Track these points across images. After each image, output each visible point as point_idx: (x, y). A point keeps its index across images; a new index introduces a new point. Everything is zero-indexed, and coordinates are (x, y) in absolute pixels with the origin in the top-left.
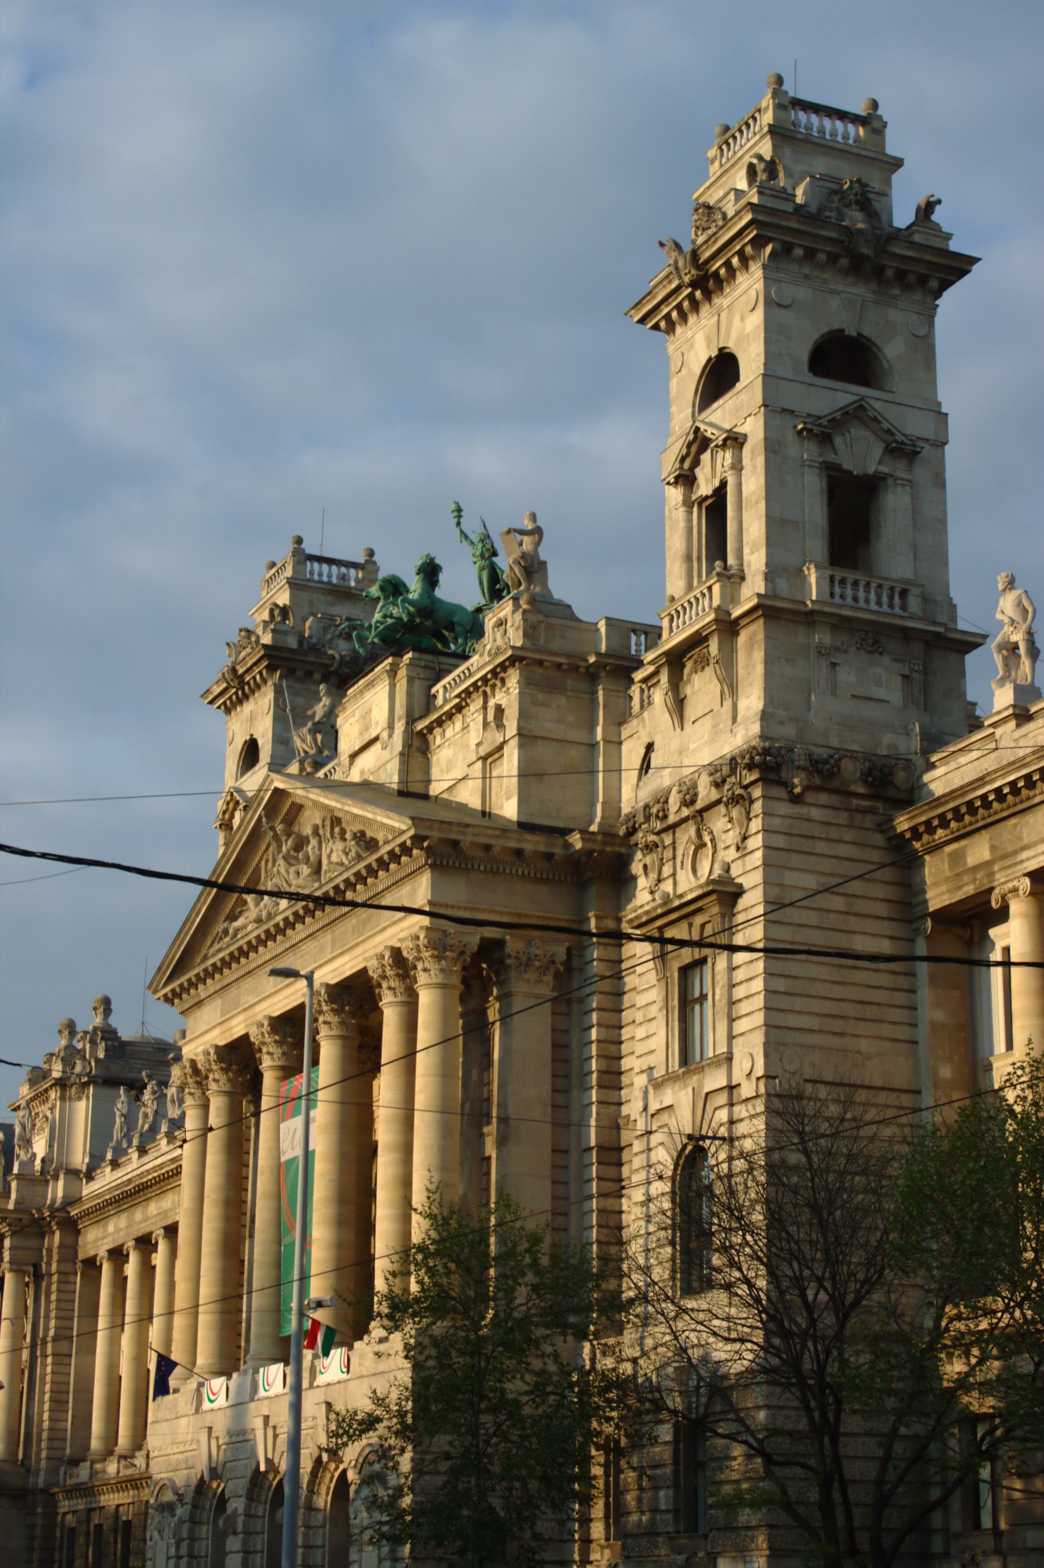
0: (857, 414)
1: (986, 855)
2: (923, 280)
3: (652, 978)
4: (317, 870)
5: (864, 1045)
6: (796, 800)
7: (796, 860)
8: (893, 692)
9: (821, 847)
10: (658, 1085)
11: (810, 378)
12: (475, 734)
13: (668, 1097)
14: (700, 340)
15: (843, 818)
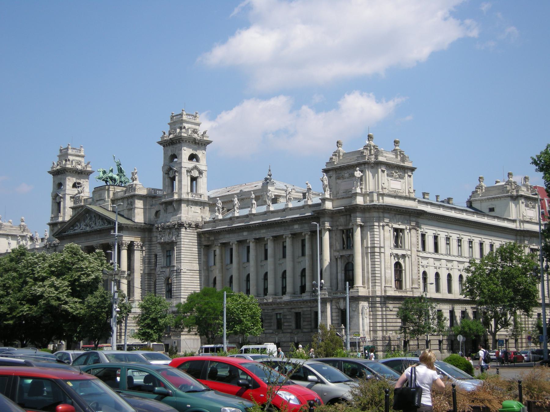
0: (195, 168)
1: (213, 239)
2: (205, 144)
3: (161, 251)
4: (95, 224)
5: (194, 264)
6: (186, 229)
7: (186, 238)
8: (199, 211)
9: (189, 235)
10: (162, 268)
11: (188, 162)
12: (126, 205)
13: (164, 270)
14: (170, 150)
15: (192, 231)
